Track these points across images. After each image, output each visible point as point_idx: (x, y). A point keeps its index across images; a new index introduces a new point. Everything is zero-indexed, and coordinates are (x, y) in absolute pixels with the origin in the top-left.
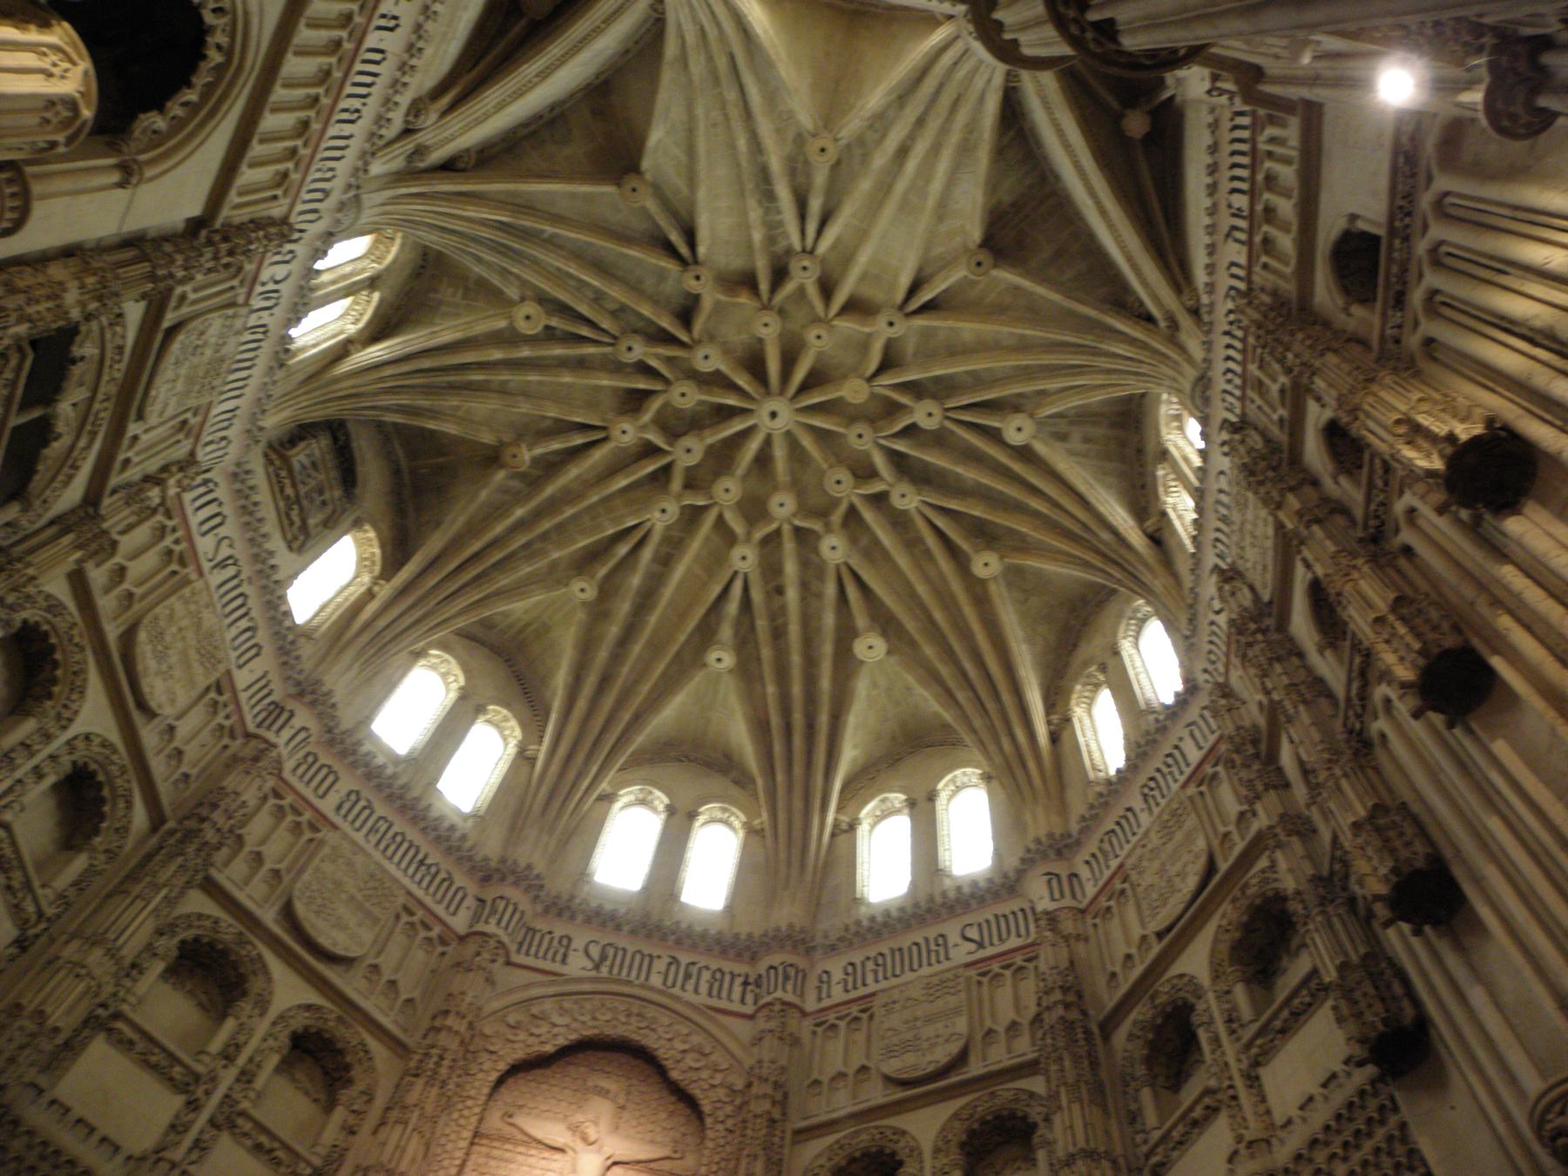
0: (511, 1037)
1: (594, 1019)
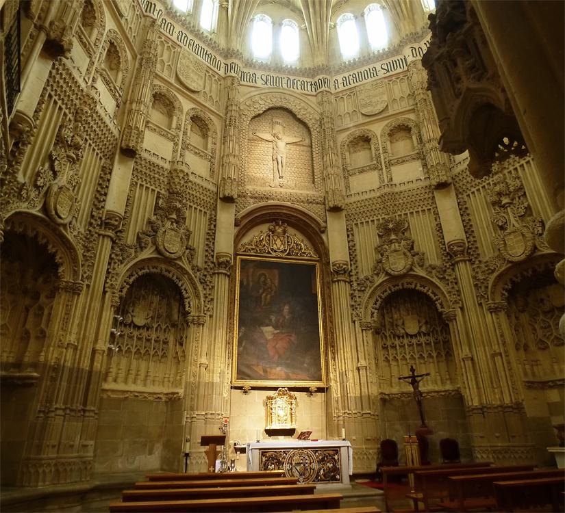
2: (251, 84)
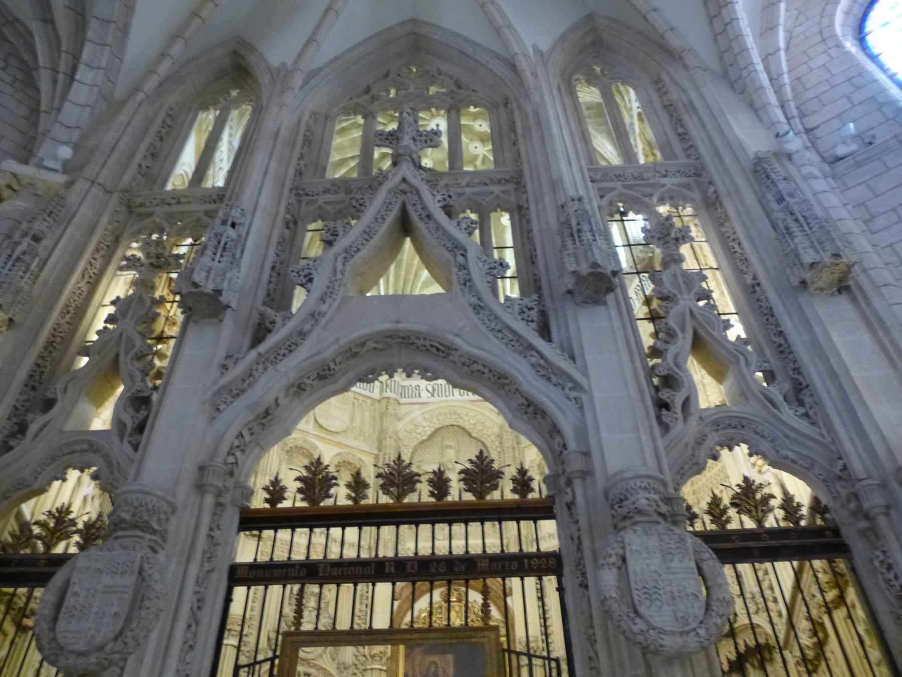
2: (413, 400)
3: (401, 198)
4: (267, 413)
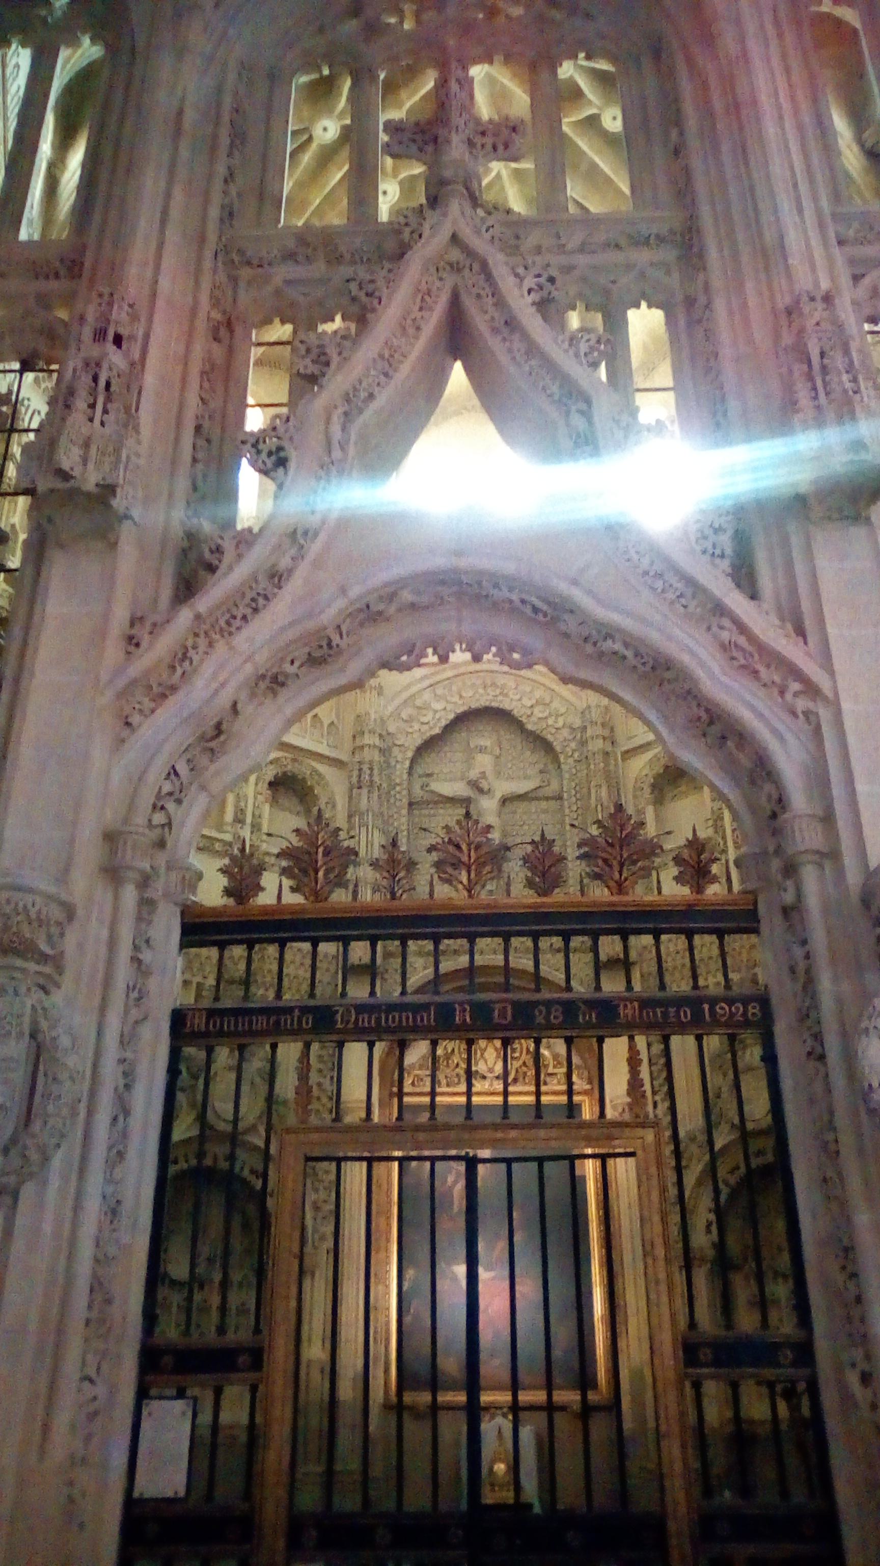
0: (410, 730)
1: (461, 697)
3: (450, 280)
4: (218, 729)
